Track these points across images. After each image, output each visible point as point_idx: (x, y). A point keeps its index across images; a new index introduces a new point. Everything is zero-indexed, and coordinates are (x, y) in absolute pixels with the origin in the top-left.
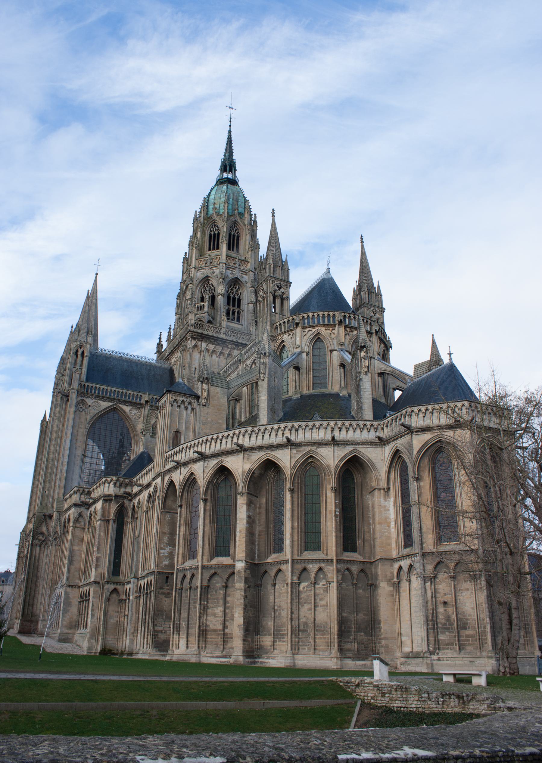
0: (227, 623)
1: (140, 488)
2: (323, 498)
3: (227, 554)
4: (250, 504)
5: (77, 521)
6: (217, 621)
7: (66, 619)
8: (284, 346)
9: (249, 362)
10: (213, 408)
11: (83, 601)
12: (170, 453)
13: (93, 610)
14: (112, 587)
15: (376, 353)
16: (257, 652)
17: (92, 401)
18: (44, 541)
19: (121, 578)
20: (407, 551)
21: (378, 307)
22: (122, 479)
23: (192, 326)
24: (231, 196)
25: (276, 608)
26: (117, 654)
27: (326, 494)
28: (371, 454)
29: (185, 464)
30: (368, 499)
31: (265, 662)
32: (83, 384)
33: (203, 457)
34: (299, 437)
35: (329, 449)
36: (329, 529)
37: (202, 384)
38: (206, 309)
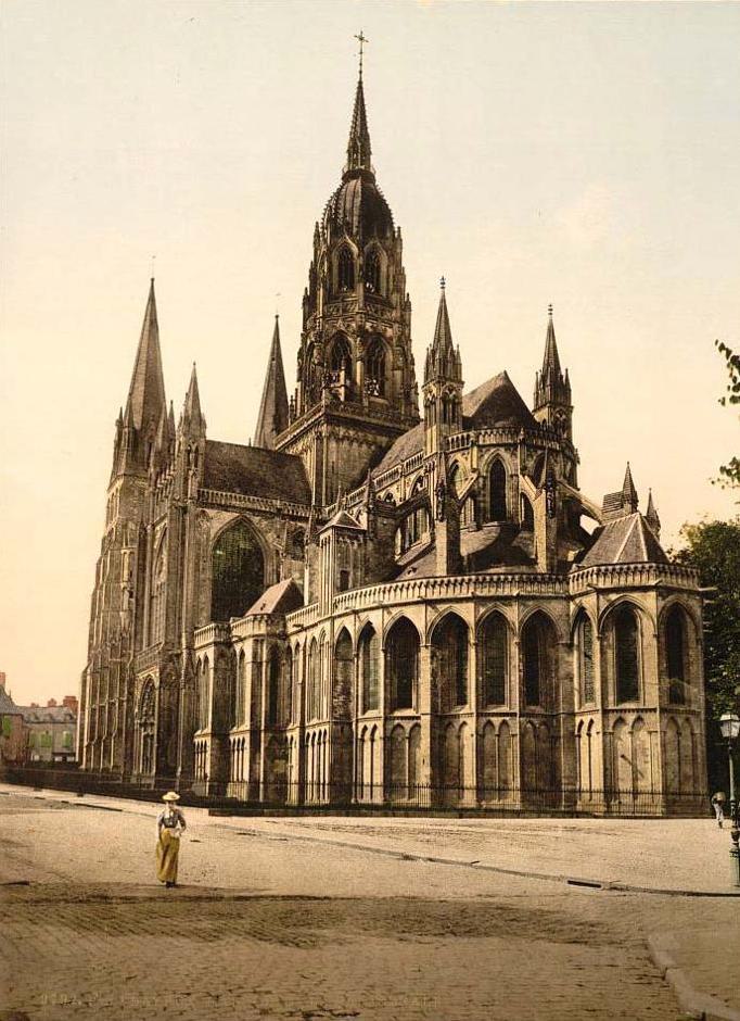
5: (216, 661)
8: (457, 467)
9: (413, 477)
21: (565, 406)
36: (513, 683)
38: (342, 382)
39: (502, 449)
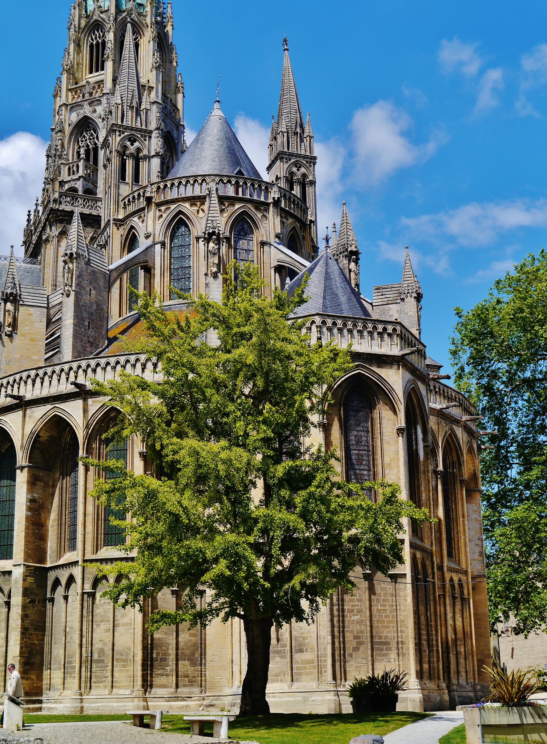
10: (23, 338)
15: (272, 235)
25: (68, 630)
31: (52, 708)
37: (5, 303)
39: (187, 205)
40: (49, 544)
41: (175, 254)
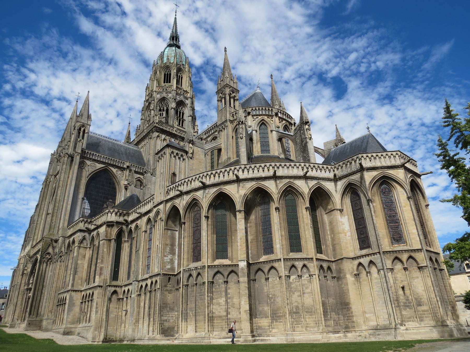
0: (229, 310)
1: (139, 215)
2: (300, 215)
3: (226, 257)
4: (247, 218)
5: (81, 242)
6: (221, 309)
7: (71, 317)
11: (85, 302)
12: (172, 187)
13: (97, 308)
14: (113, 289)
16: (256, 331)
17: (90, 163)
18: (50, 259)
19: (119, 283)
20: (364, 252)
22: (121, 211)
23: (157, 123)
24: (178, 54)
25: (270, 296)
26: (116, 341)
27: (302, 212)
28: (329, 186)
29: (188, 193)
30: (326, 217)
31: (265, 340)
32: (84, 150)
33: (204, 187)
34: (280, 172)
35: (302, 181)
39: (266, 117)
40: (250, 252)
41: (262, 135)
